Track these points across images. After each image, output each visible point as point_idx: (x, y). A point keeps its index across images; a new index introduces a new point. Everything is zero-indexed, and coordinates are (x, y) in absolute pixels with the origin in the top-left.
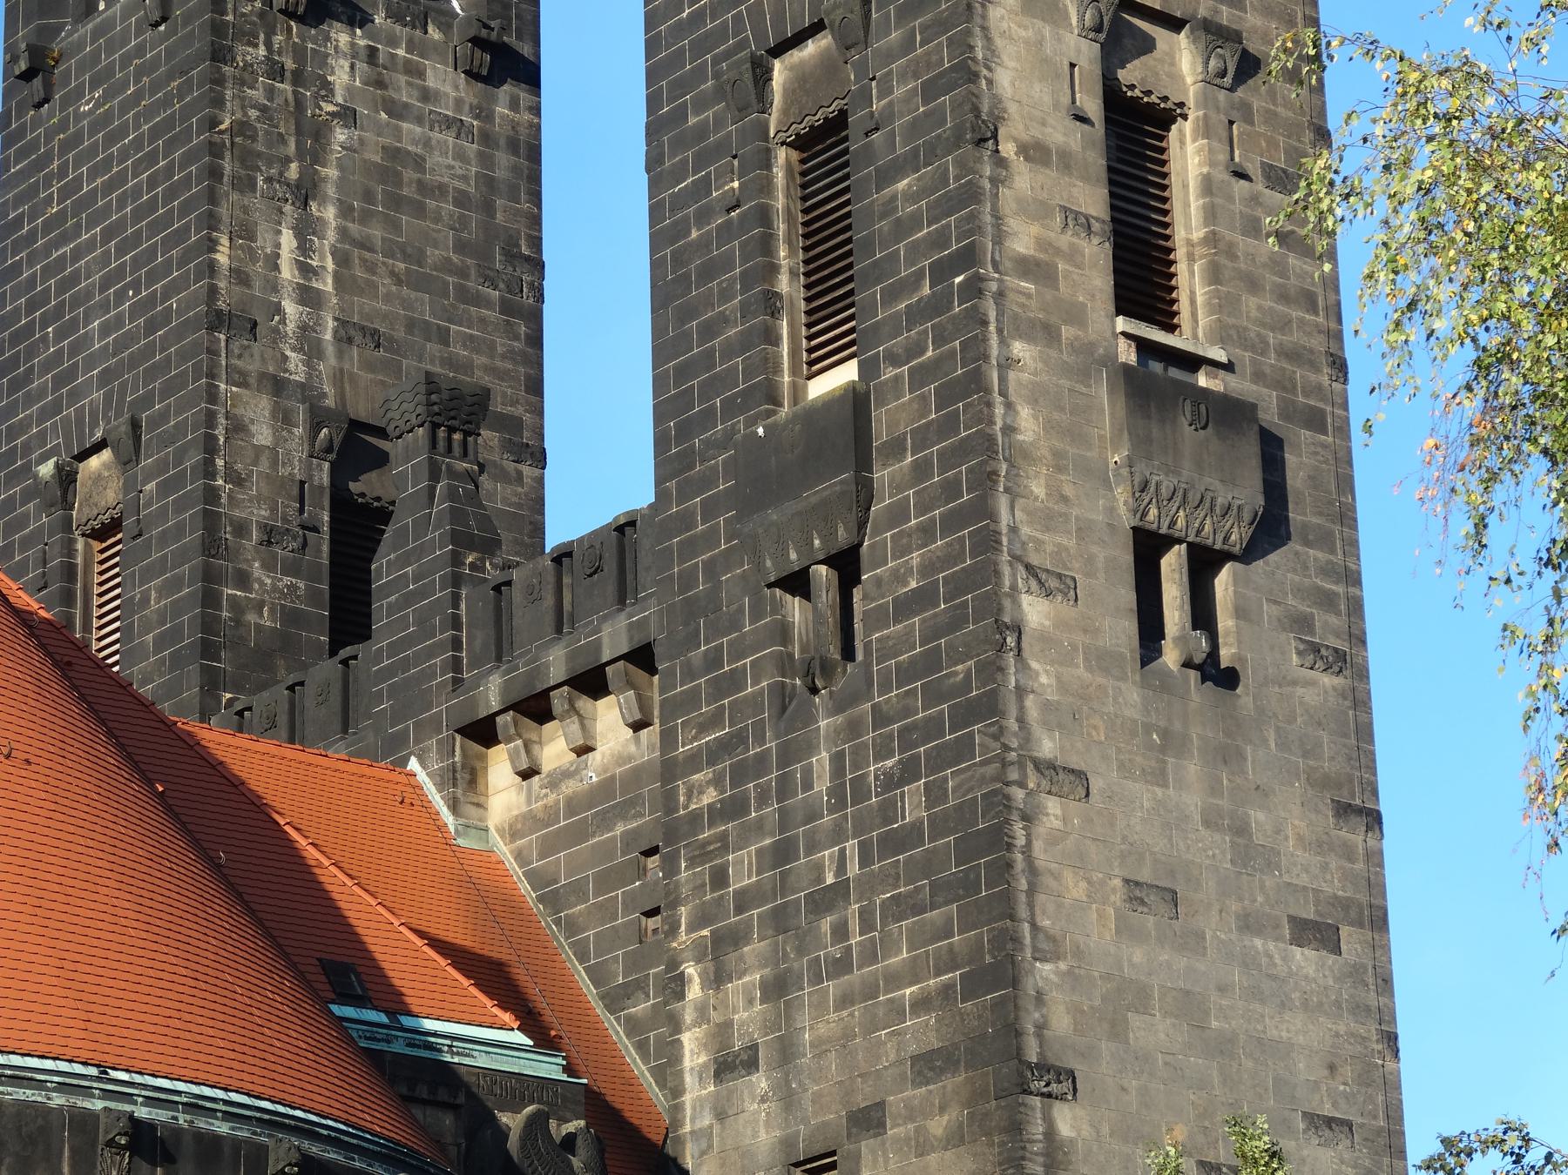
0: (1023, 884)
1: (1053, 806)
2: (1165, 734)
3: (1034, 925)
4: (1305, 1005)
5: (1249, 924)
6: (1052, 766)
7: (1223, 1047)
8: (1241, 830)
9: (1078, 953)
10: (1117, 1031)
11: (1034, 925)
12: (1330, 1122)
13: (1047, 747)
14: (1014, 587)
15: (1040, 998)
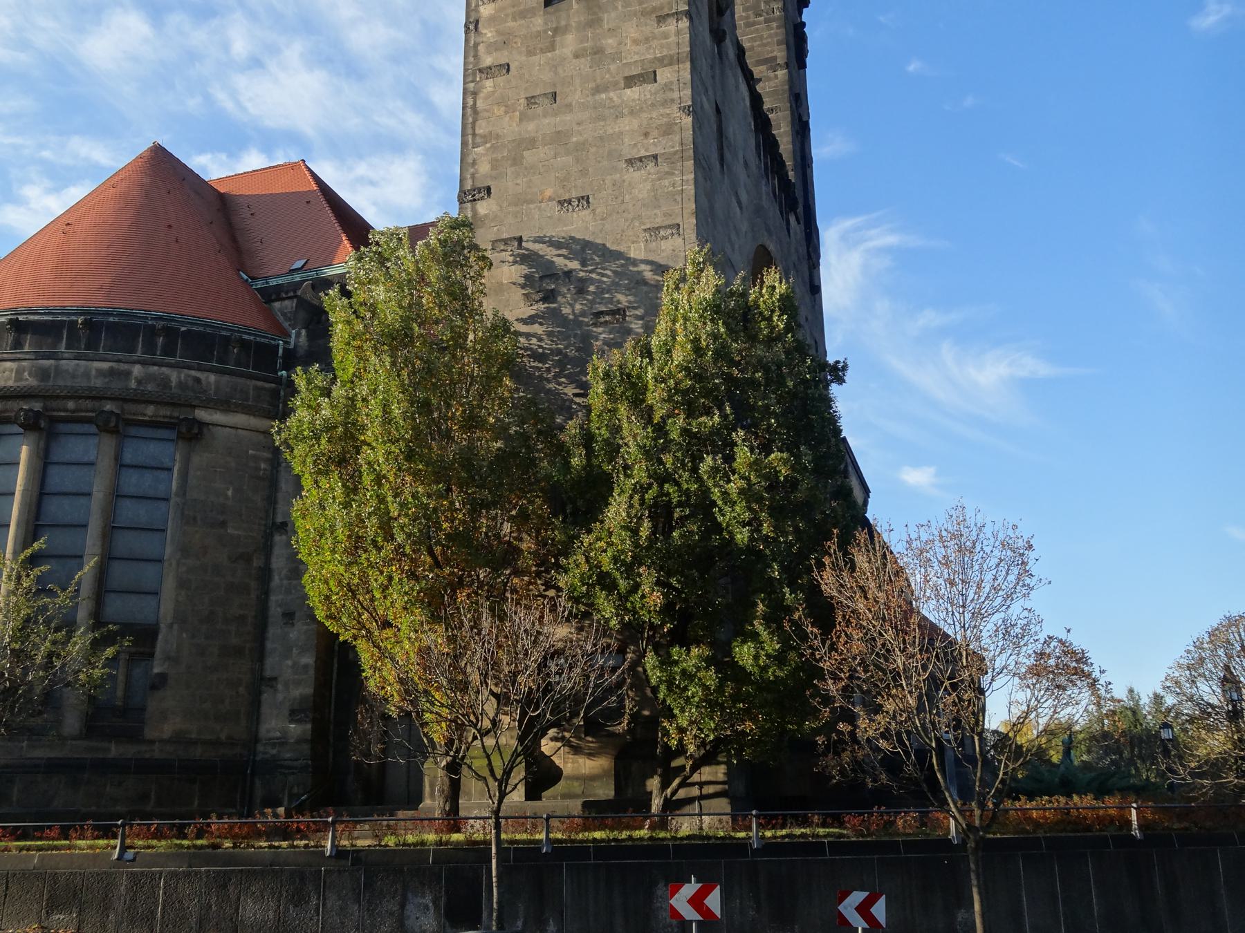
0: (470, 120)
1: (489, 84)
2: (556, 31)
3: (474, 135)
4: (632, 113)
5: (597, 90)
6: (490, 68)
7: (581, 146)
8: (598, 51)
9: (498, 137)
10: (516, 161)
11: (474, 135)
12: (640, 159)
13: (488, 61)
14: (477, 6)
15: (474, 163)
